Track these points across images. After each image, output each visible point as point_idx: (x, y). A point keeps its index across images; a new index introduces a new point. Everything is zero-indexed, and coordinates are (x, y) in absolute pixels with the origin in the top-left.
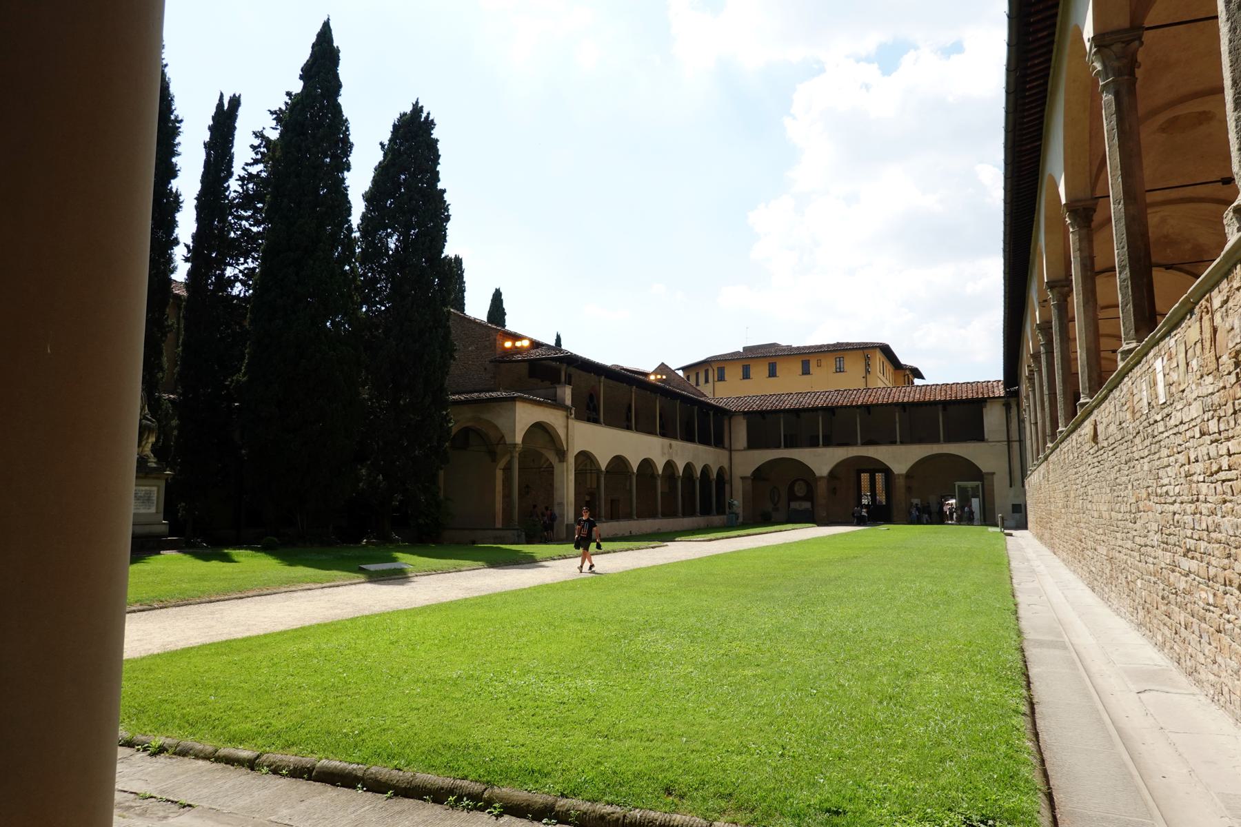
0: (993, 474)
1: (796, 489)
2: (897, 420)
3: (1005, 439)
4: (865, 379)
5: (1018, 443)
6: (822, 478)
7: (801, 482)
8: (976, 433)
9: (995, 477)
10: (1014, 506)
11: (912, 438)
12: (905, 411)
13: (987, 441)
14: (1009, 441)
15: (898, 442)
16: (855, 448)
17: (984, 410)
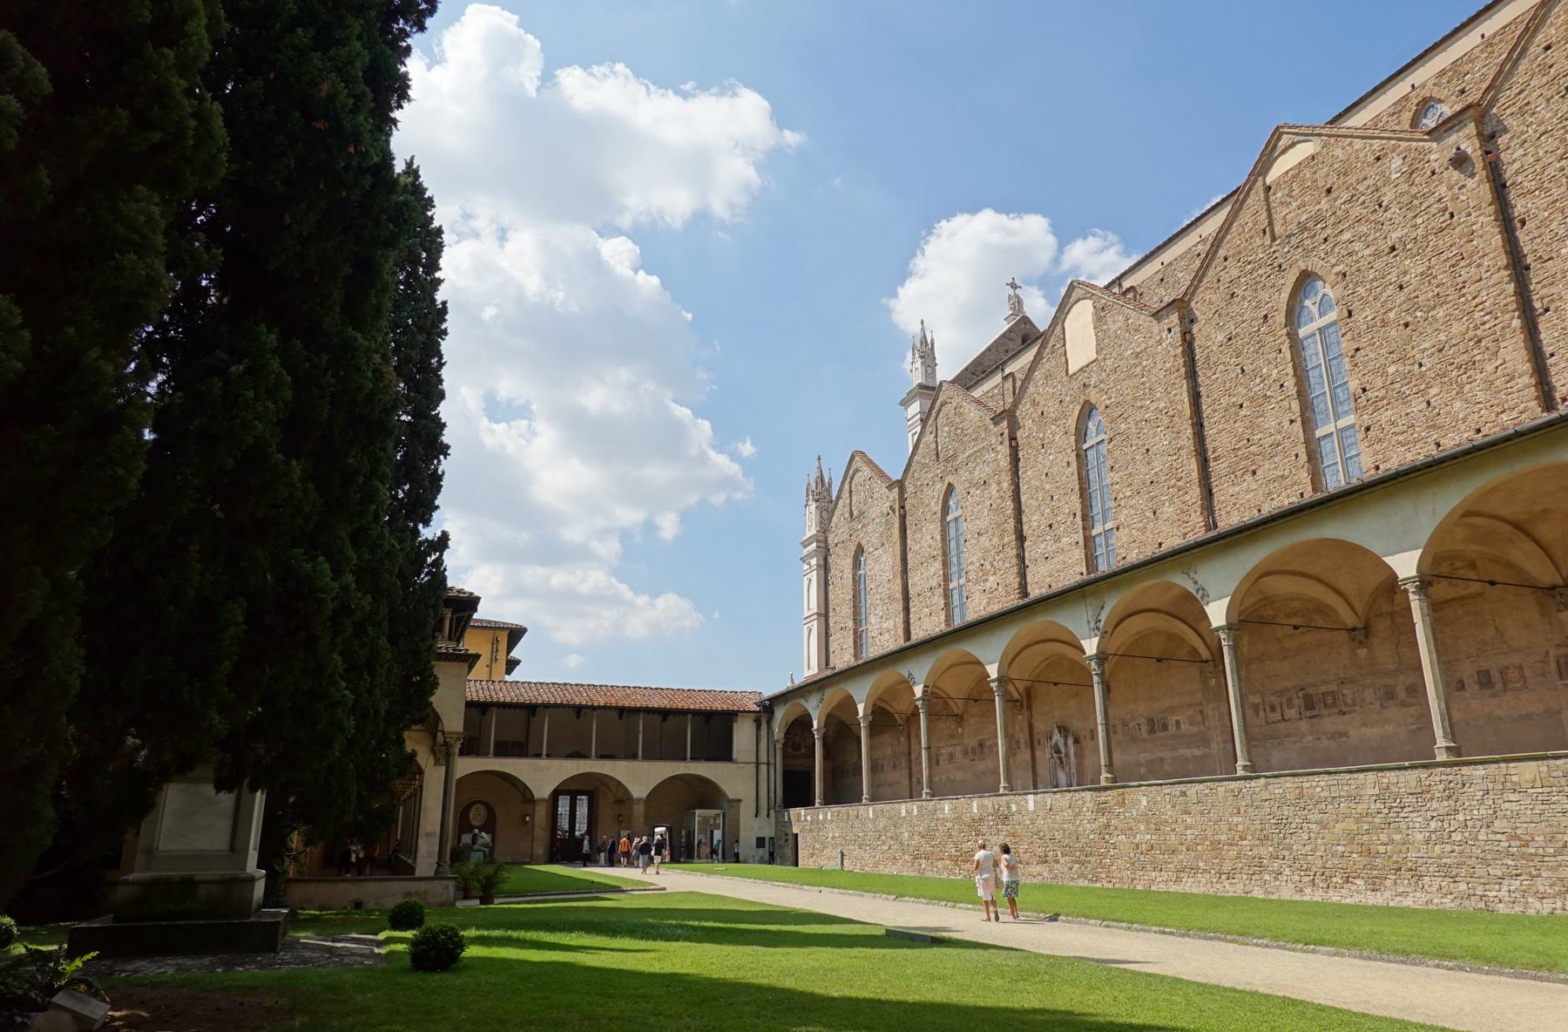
0: (740, 801)
1: (471, 815)
2: (641, 728)
3: (754, 760)
4: (488, 669)
5: (766, 766)
6: (542, 800)
7: (478, 805)
8: (721, 750)
9: (742, 805)
10: (758, 838)
11: (654, 753)
12: (620, 718)
13: (736, 762)
14: (758, 764)
15: (544, 756)
16: (588, 762)
17: (735, 725)
